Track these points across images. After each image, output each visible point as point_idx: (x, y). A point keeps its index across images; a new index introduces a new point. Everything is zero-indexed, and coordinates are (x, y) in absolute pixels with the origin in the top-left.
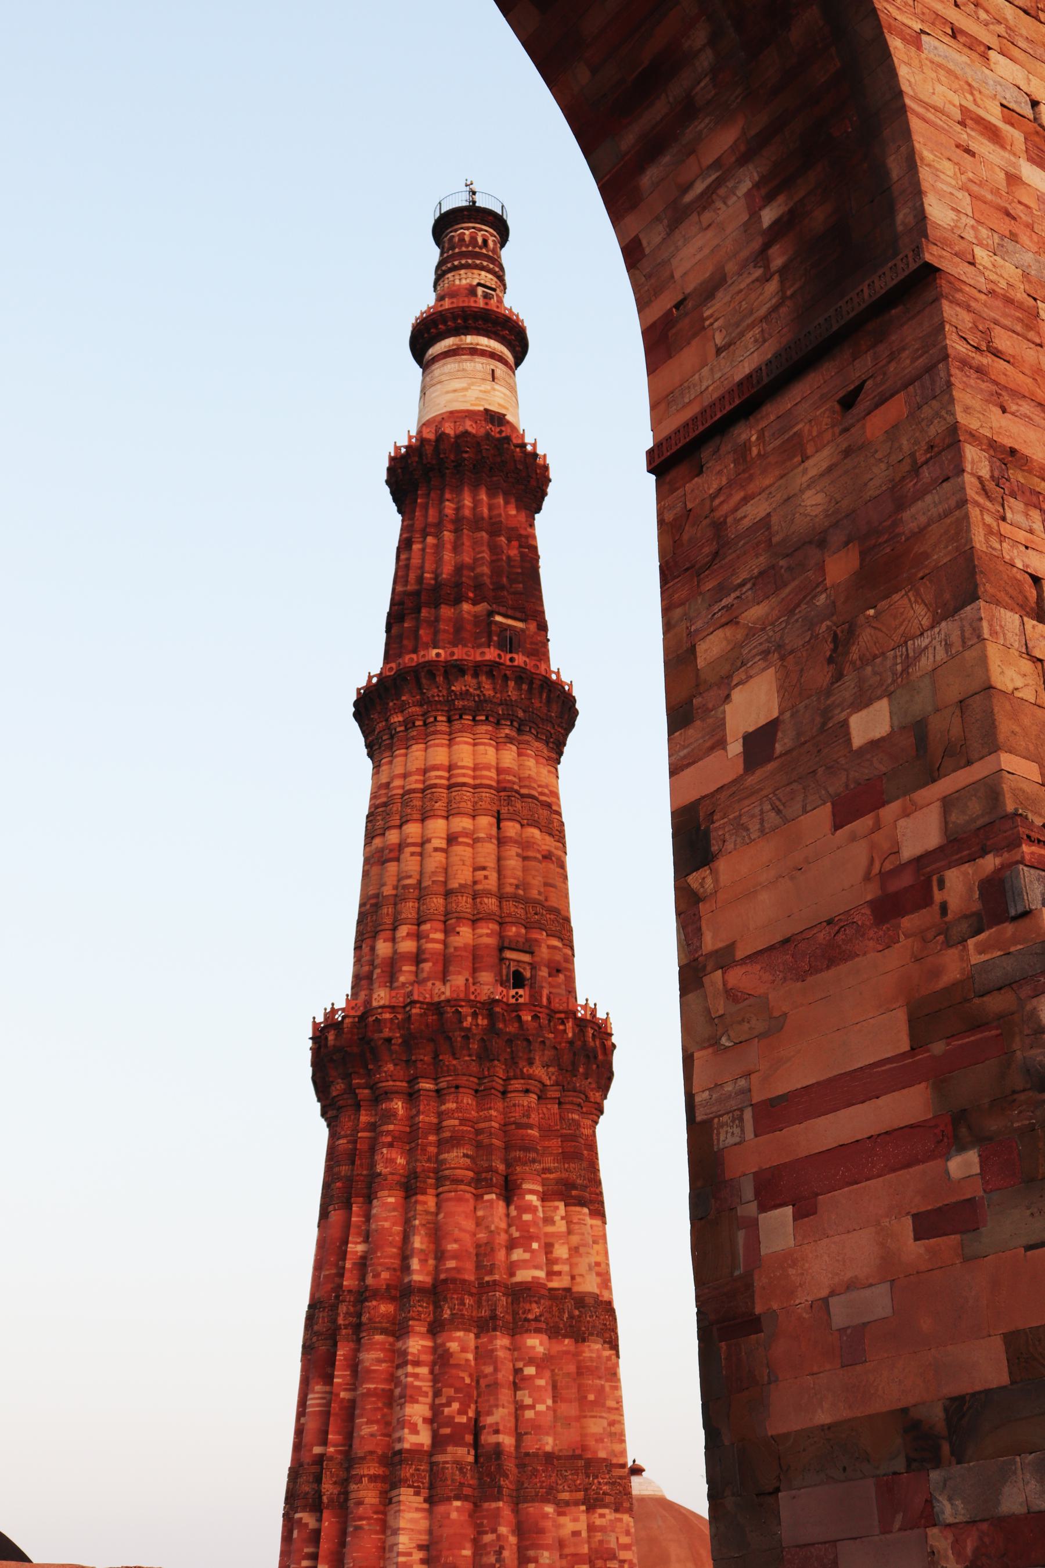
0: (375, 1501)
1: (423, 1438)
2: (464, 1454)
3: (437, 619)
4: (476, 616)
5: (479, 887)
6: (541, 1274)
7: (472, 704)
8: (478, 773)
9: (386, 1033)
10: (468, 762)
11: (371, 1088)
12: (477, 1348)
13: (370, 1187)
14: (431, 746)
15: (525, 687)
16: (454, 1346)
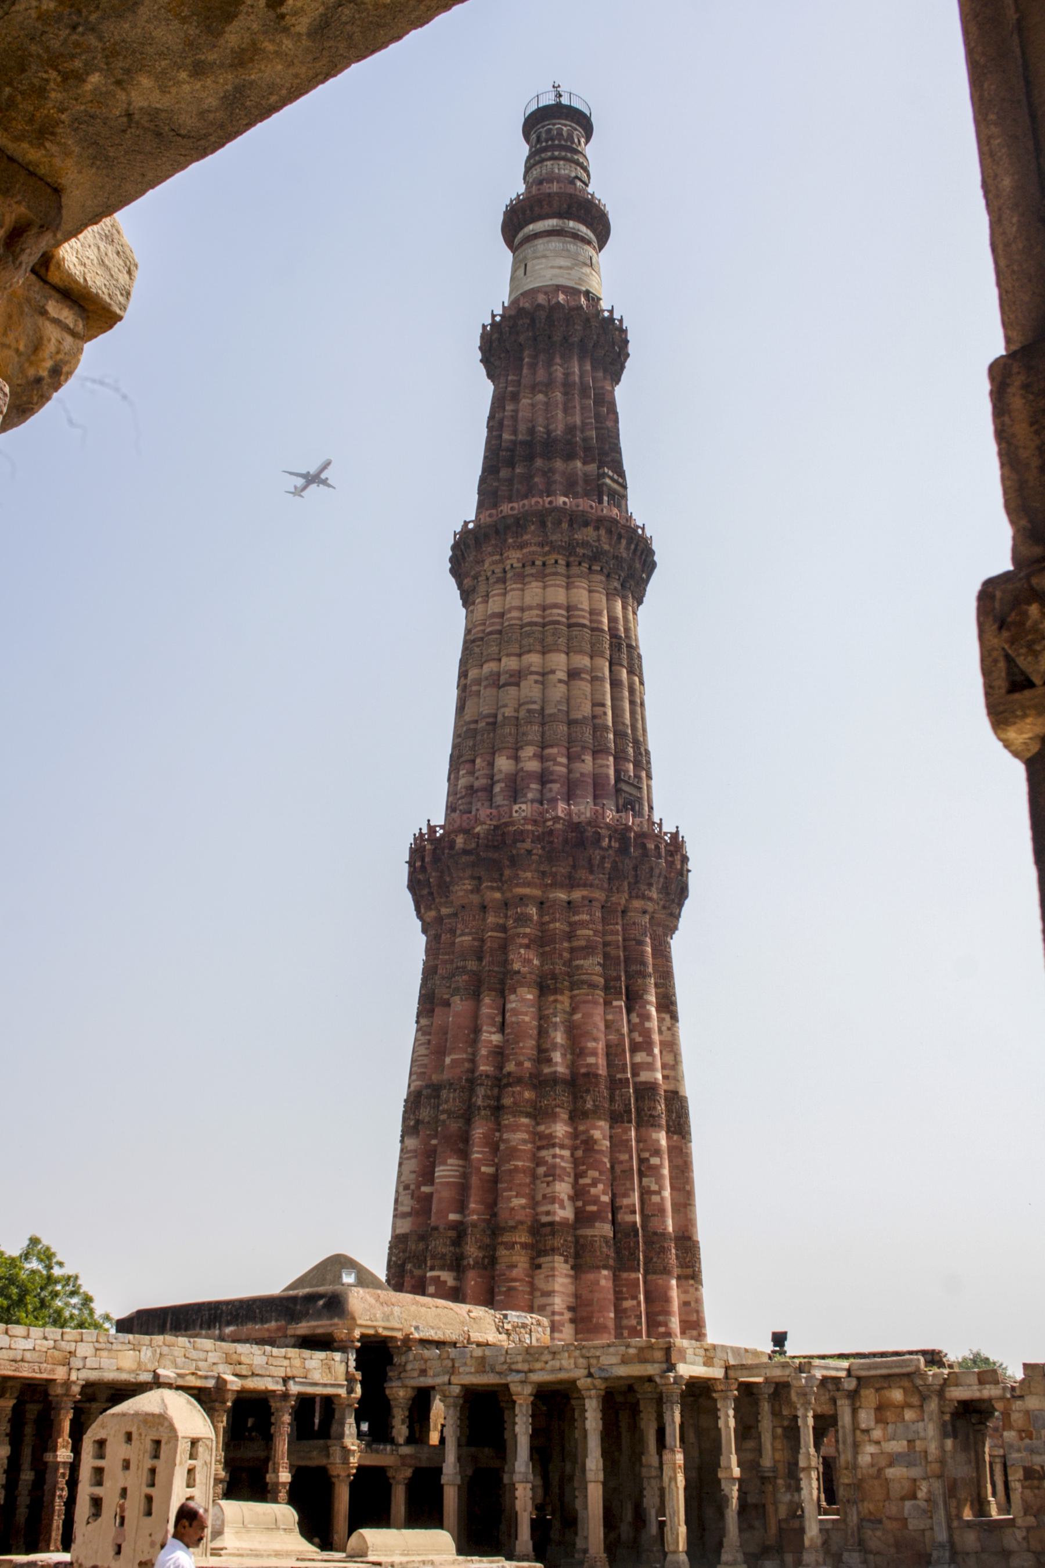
0: (527, 1265)
1: (564, 1213)
2: (606, 1229)
3: (552, 471)
4: (585, 475)
5: (597, 721)
6: (659, 1076)
7: (590, 554)
8: (594, 617)
9: (528, 845)
10: (585, 606)
11: (503, 893)
12: (611, 1137)
13: (502, 982)
14: (552, 585)
15: (633, 547)
16: (597, 1134)
